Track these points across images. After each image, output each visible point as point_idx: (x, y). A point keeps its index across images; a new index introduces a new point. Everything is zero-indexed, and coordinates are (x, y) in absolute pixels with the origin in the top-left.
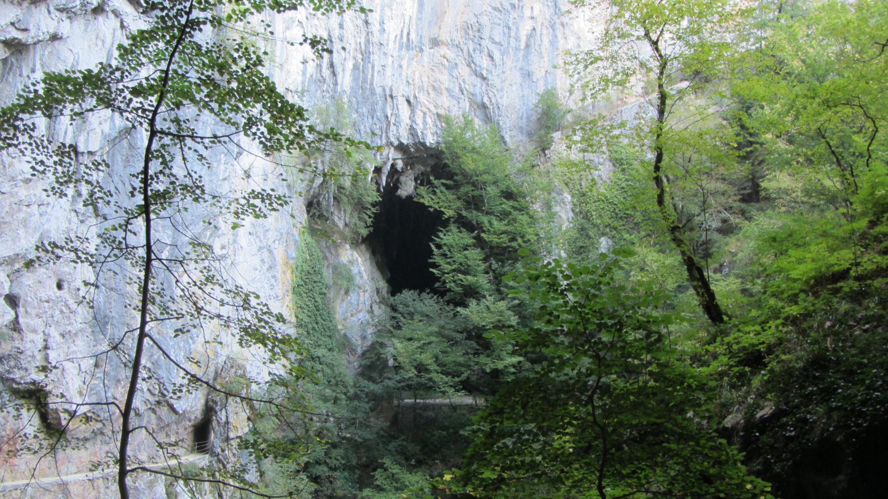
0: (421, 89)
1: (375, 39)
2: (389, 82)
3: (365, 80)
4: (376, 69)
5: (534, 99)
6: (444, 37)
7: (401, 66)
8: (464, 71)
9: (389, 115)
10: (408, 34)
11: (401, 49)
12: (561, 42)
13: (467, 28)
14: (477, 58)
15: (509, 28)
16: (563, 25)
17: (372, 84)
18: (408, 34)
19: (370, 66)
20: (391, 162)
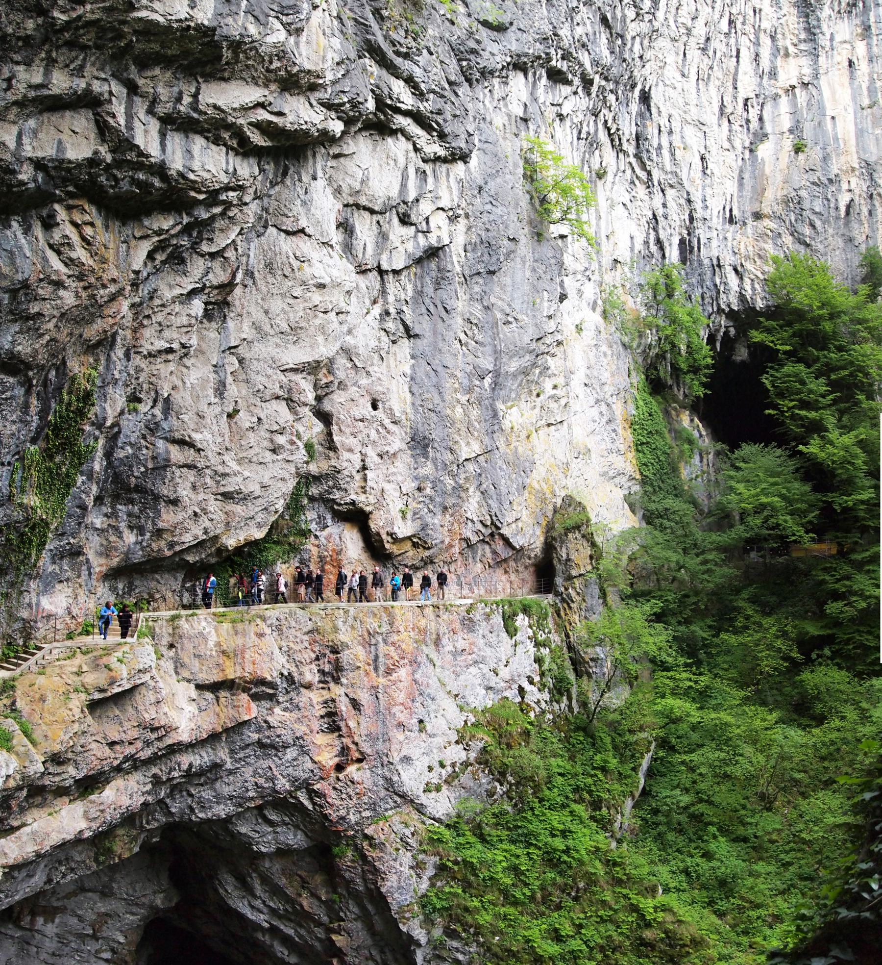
0: (747, 257)
1: (698, 215)
2: (715, 253)
4: (702, 242)
5: (856, 261)
6: (766, 210)
8: (788, 240)
10: (731, 210)
13: (787, 201)
17: (699, 256)
18: (731, 210)
19: (696, 240)
20: (723, 330)
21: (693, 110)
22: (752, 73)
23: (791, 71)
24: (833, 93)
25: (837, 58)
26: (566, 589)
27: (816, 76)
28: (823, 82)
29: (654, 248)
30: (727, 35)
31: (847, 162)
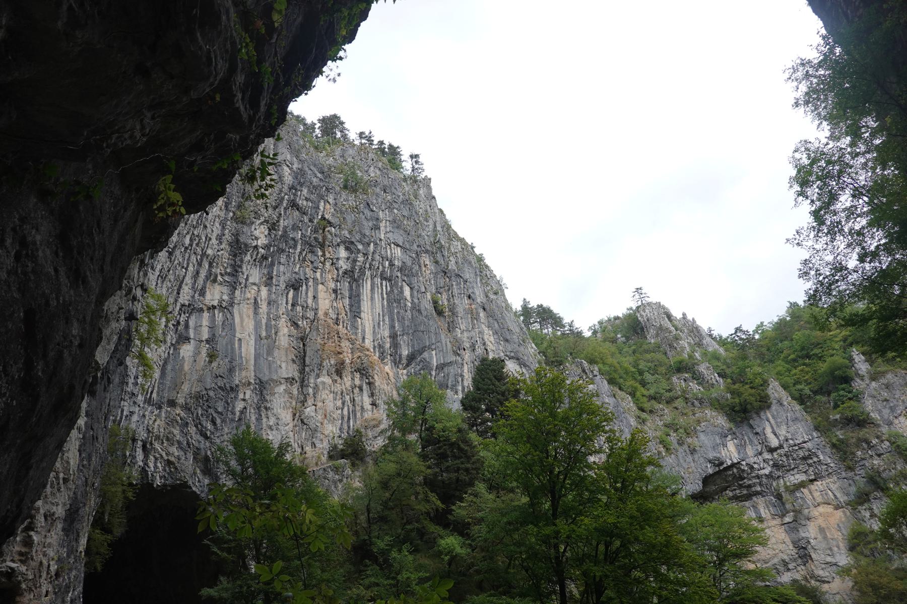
0: (158, 438)
2: (133, 426)
4: (125, 413)
7: (144, 416)
8: (192, 430)
9: (128, 454)
11: (144, 403)
12: (265, 420)
13: (198, 397)
14: (203, 419)
15: (228, 404)
18: (152, 392)
22: (190, 286)
24: (242, 321)
27: (232, 304)
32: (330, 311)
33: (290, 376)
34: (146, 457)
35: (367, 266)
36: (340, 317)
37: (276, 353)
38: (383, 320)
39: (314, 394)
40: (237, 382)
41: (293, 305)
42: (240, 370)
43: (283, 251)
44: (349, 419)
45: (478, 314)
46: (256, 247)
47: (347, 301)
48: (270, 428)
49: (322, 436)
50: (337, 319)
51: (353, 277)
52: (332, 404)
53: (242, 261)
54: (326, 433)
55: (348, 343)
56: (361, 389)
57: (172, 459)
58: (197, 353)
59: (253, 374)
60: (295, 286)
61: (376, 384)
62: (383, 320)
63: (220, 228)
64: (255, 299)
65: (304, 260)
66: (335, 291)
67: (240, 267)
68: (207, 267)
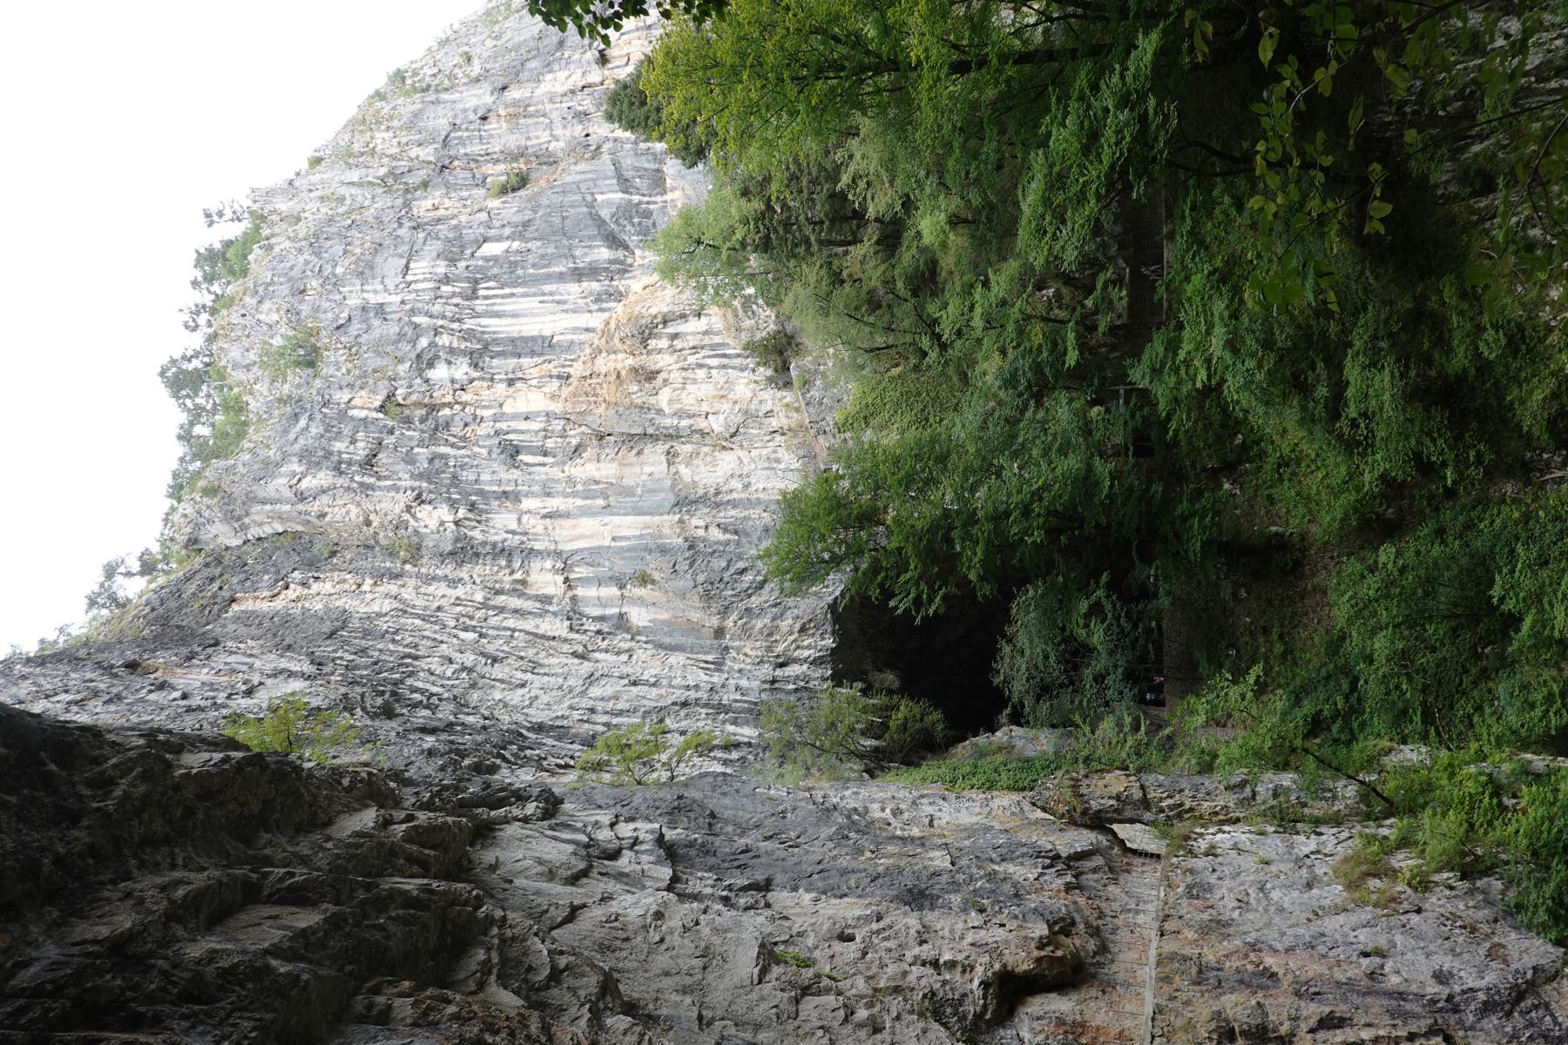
0: (769, 649)
2: (756, 684)
3: (750, 711)
4: (739, 697)
7: (740, 671)
8: (755, 601)
11: (720, 671)
12: (735, 495)
13: (707, 597)
16: (717, 494)
17: (756, 704)
21: (571, 682)
22: (538, 621)
23: (545, 580)
25: (540, 529)
26: (1162, 811)
27: (558, 554)
28: (567, 547)
29: (735, 755)
30: (481, 635)
31: (671, 527)
32: (546, 390)
33: (663, 458)
34: (796, 661)
35: (456, 326)
36: (555, 372)
37: (628, 482)
38: (551, 294)
39: (690, 417)
40: (680, 540)
41: (545, 455)
42: (660, 536)
43: (455, 477)
44: (724, 356)
45: (515, 103)
46: (457, 523)
47: (526, 361)
48: (747, 486)
49: (755, 401)
50: (559, 377)
51: (481, 351)
52: (704, 386)
53: (484, 543)
54: (749, 395)
55: (600, 361)
56: (675, 336)
57: (798, 626)
58: (641, 602)
59: (666, 517)
60: (512, 452)
61: (665, 310)
62: (551, 294)
63: (435, 585)
64: (545, 517)
65: (464, 438)
66: (511, 382)
67: (494, 545)
68: (503, 597)
